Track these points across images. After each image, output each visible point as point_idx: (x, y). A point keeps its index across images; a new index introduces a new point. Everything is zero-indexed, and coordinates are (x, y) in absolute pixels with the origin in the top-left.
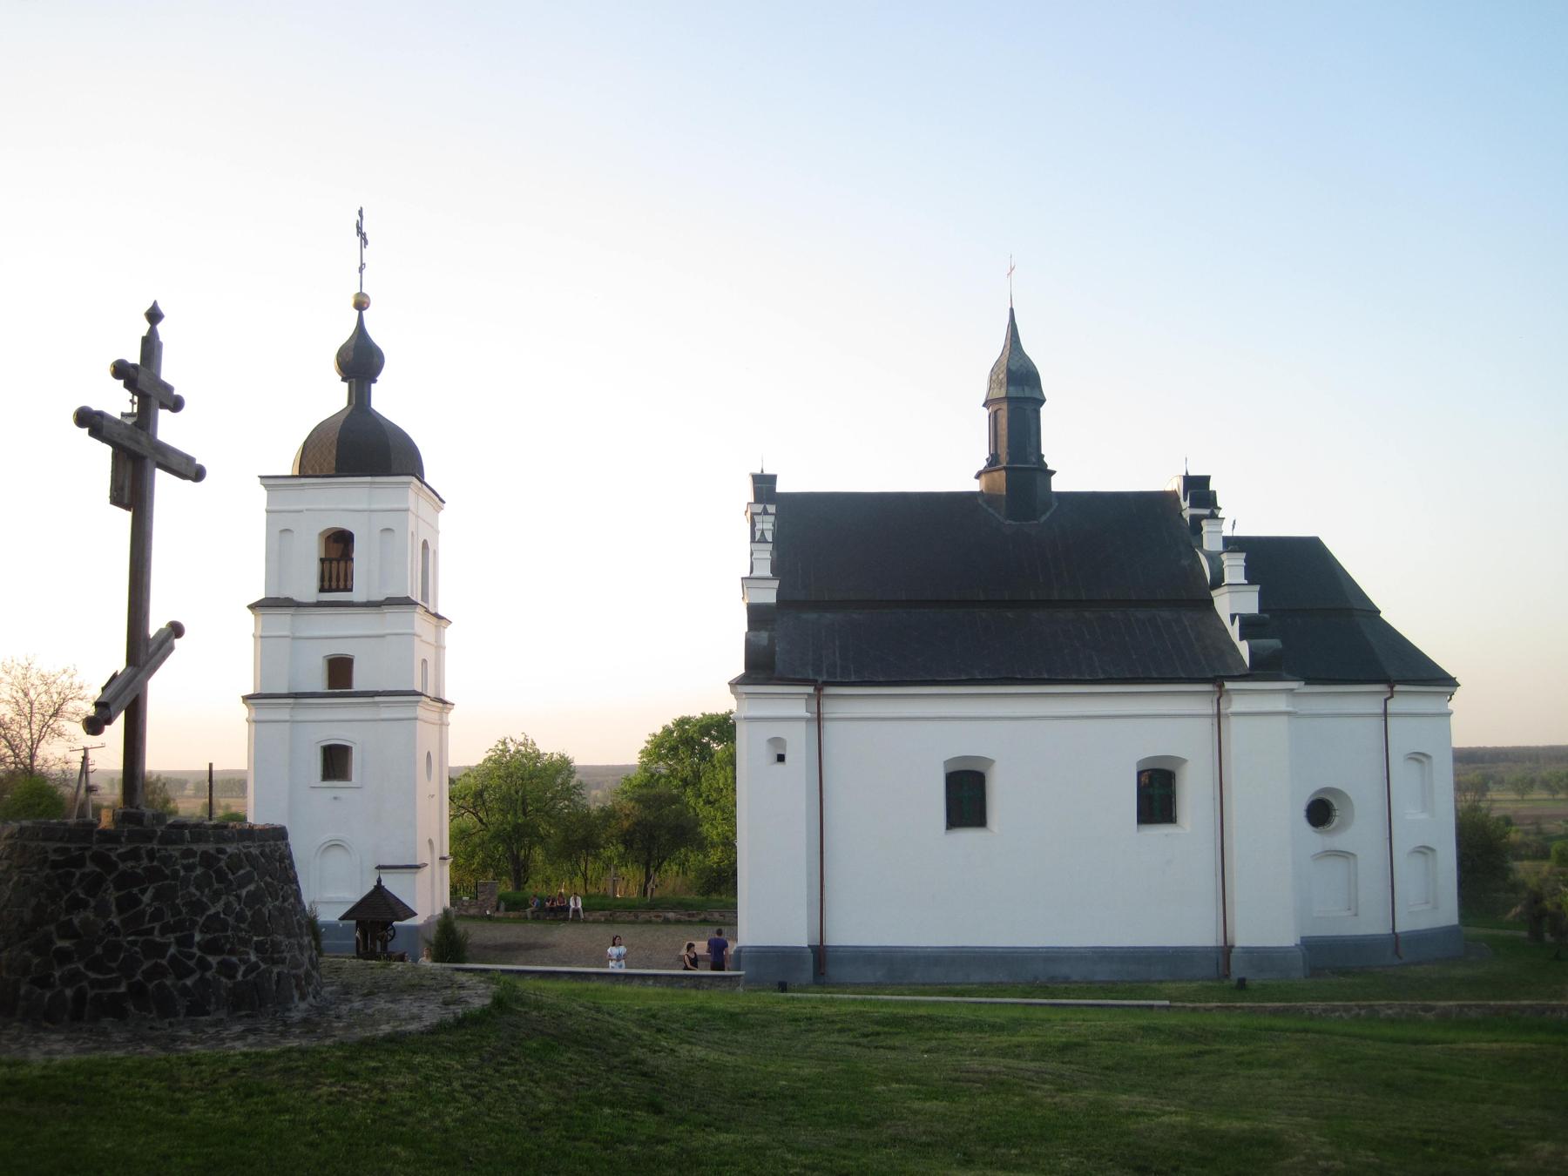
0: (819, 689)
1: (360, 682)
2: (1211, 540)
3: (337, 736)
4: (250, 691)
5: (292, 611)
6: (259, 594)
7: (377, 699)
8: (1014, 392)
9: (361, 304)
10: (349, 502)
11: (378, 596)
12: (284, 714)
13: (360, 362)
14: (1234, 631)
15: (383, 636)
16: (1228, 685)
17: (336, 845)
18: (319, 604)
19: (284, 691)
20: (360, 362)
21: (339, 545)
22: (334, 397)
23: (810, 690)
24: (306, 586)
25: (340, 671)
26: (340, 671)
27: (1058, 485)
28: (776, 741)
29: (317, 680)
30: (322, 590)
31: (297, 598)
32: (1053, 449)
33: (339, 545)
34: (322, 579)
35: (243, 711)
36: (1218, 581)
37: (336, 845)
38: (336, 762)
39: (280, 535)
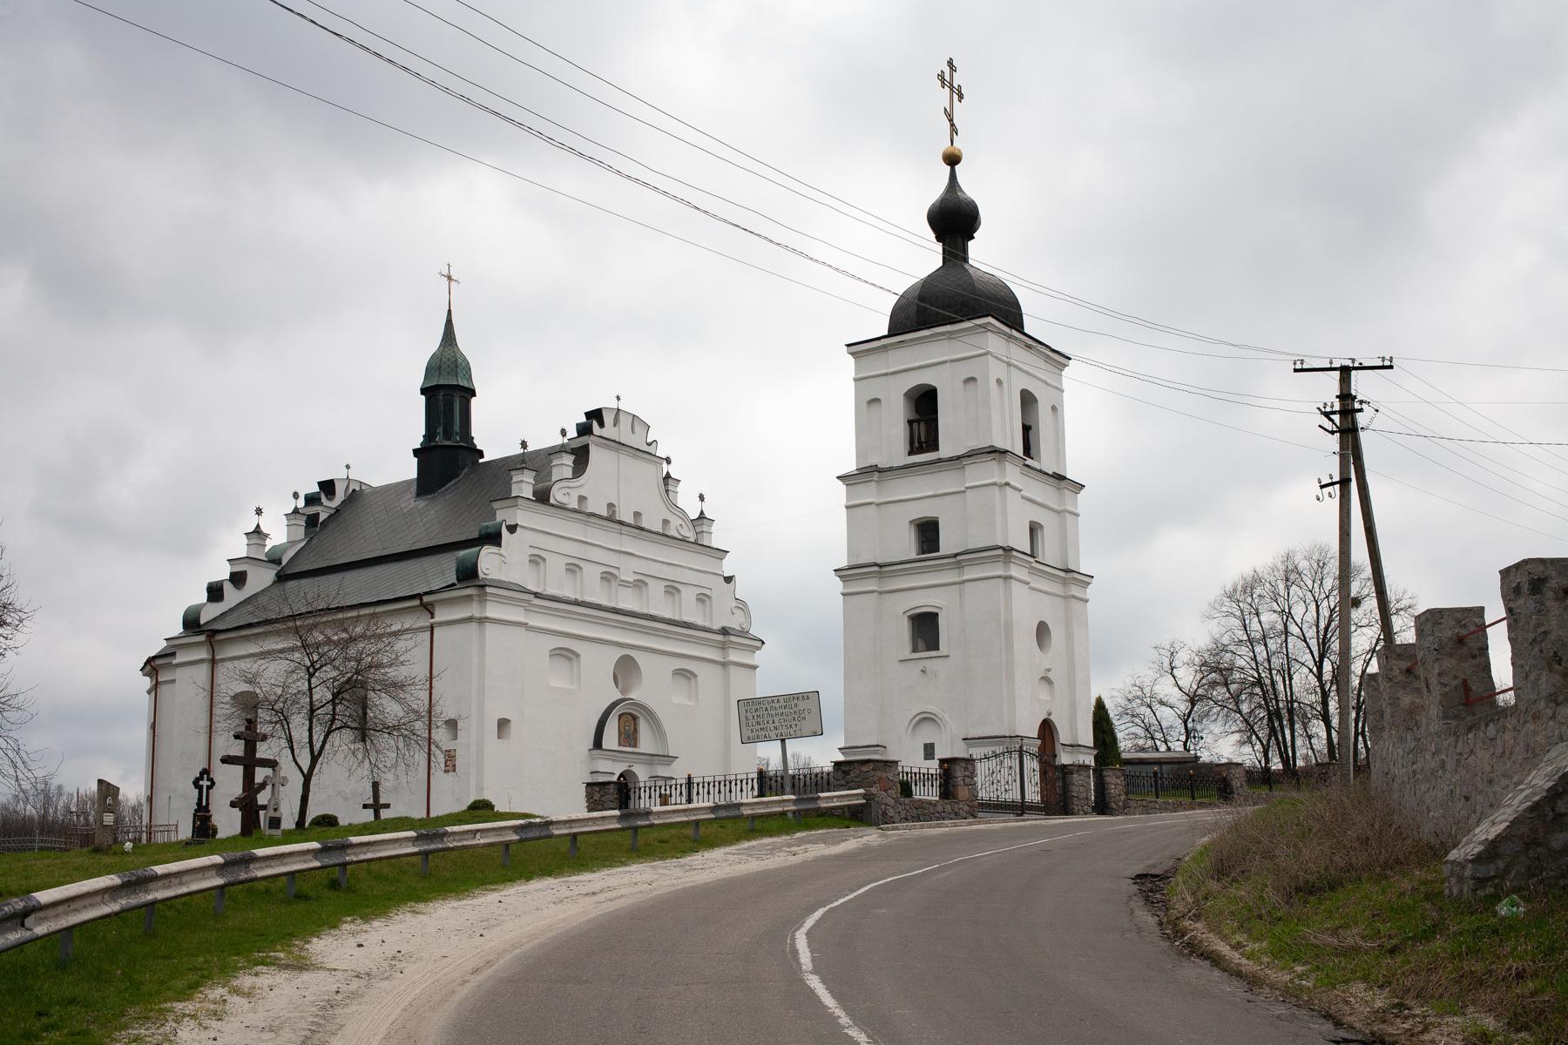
3: (924, 602)
4: (844, 563)
6: (851, 467)
9: (952, 160)
10: (935, 358)
13: (954, 221)
22: (927, 257)
24: (894, 448)
25: (928, 533)
26: (928, 533)
29: (905, 545)
30: (910, 453)
31: (895, 465)
34: (912, 443)
35: (838, 585)
38: (925, 628)
39: (869, 403)
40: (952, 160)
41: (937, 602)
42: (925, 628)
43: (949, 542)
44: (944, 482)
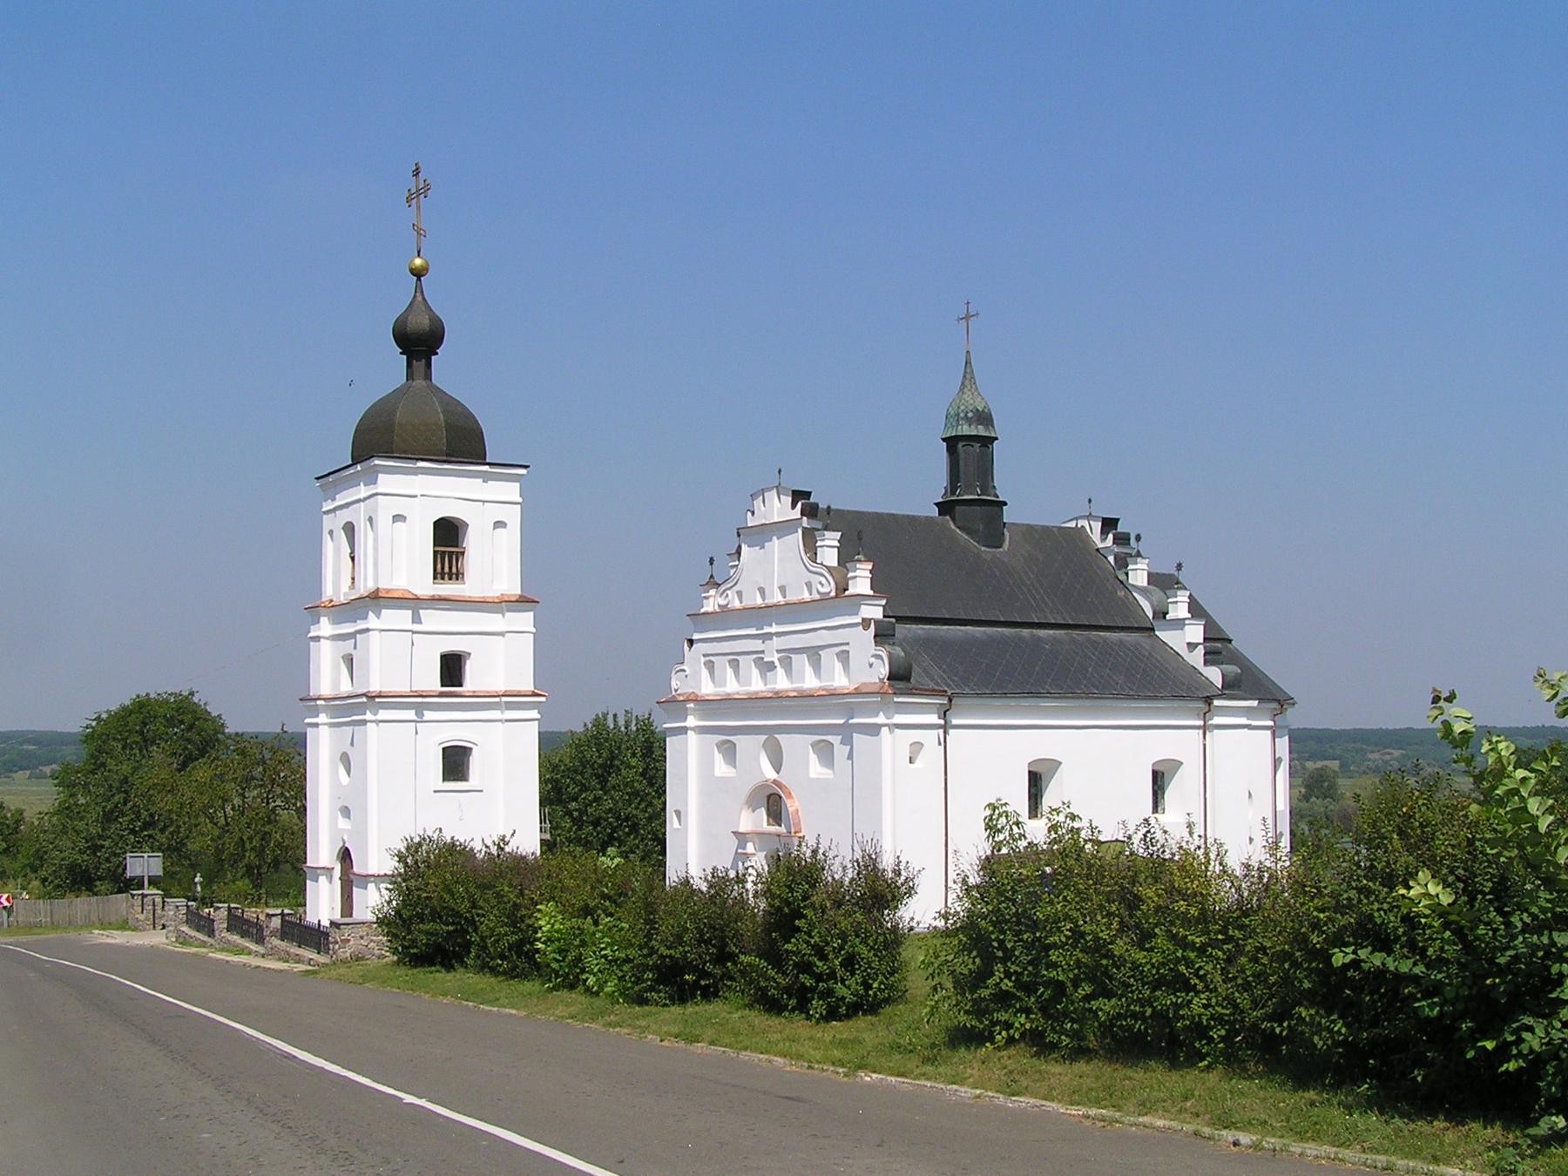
0: (950, 700)
1: (470, 684)
2: (1138, 575)
5: (412, 603)
8: (981, 431)
12: (411, 714)
14: (1196, 659)
16: (1216, 703)
19: (406, 689)
21: (448, 534)
25: (452, 668)
26: (452, 668)
27: (1008, 515)
28: (917, 747)
29: (431, 679)
32: (1004, 484)
33: (448, 534)
36: (1161, 614)
38: (455, 762)
42: (455, 762)
43: (474, 678)
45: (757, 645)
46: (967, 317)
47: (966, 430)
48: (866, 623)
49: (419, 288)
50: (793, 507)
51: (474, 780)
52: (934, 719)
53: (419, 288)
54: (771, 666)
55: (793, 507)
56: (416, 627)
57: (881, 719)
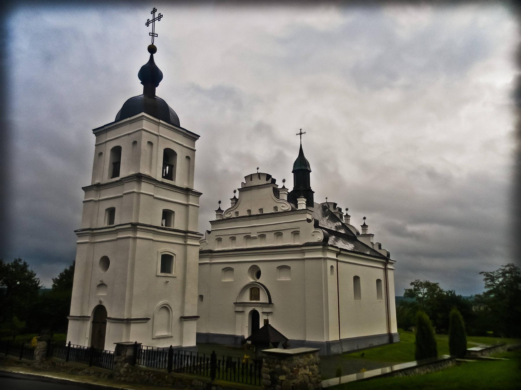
7: (189, 234)
11: (185, 185)
15: (187, 205)
17: (166, 308)
18: (162, 183)
20: (150, 75)
21: (169, 156)
23: (338, 250)
28: (332, 267)
33: (169, 156)
37: (166, 308)
40: (152, 49)
41: (175, 252)
44: (180, 198)
45: (248, 231)
46: (301, 134)
47: (303, 168)
48: (309, 221)
49: (152, 58)
50: (267, 180)
51: (173, 274)
52: (334, 256)
53: (152, 58)
54: (255, 238)
55: (267, 180)
56: (155, 196)
57: (320, 255)
